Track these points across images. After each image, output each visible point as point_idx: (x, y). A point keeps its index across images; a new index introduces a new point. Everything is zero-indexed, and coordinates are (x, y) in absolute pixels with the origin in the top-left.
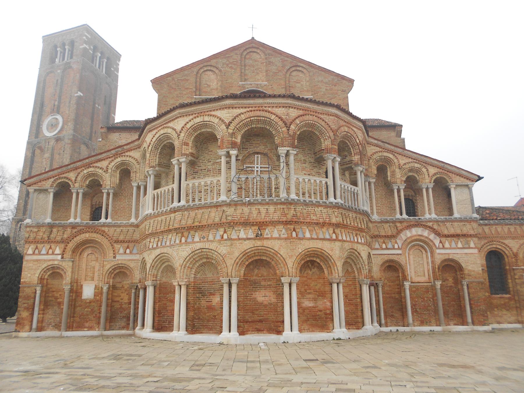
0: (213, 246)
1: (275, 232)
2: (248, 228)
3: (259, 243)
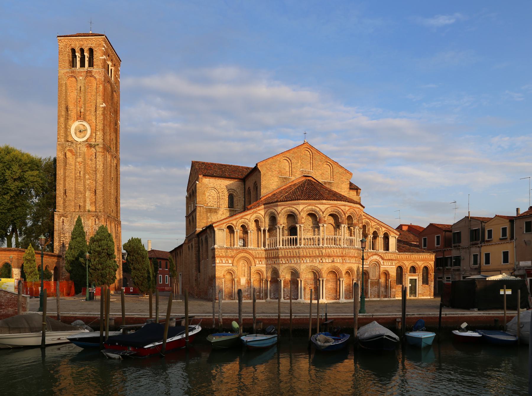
0: (316, 265)
1: (339, 260)
2: (329, 258)
3: (333, 264)
